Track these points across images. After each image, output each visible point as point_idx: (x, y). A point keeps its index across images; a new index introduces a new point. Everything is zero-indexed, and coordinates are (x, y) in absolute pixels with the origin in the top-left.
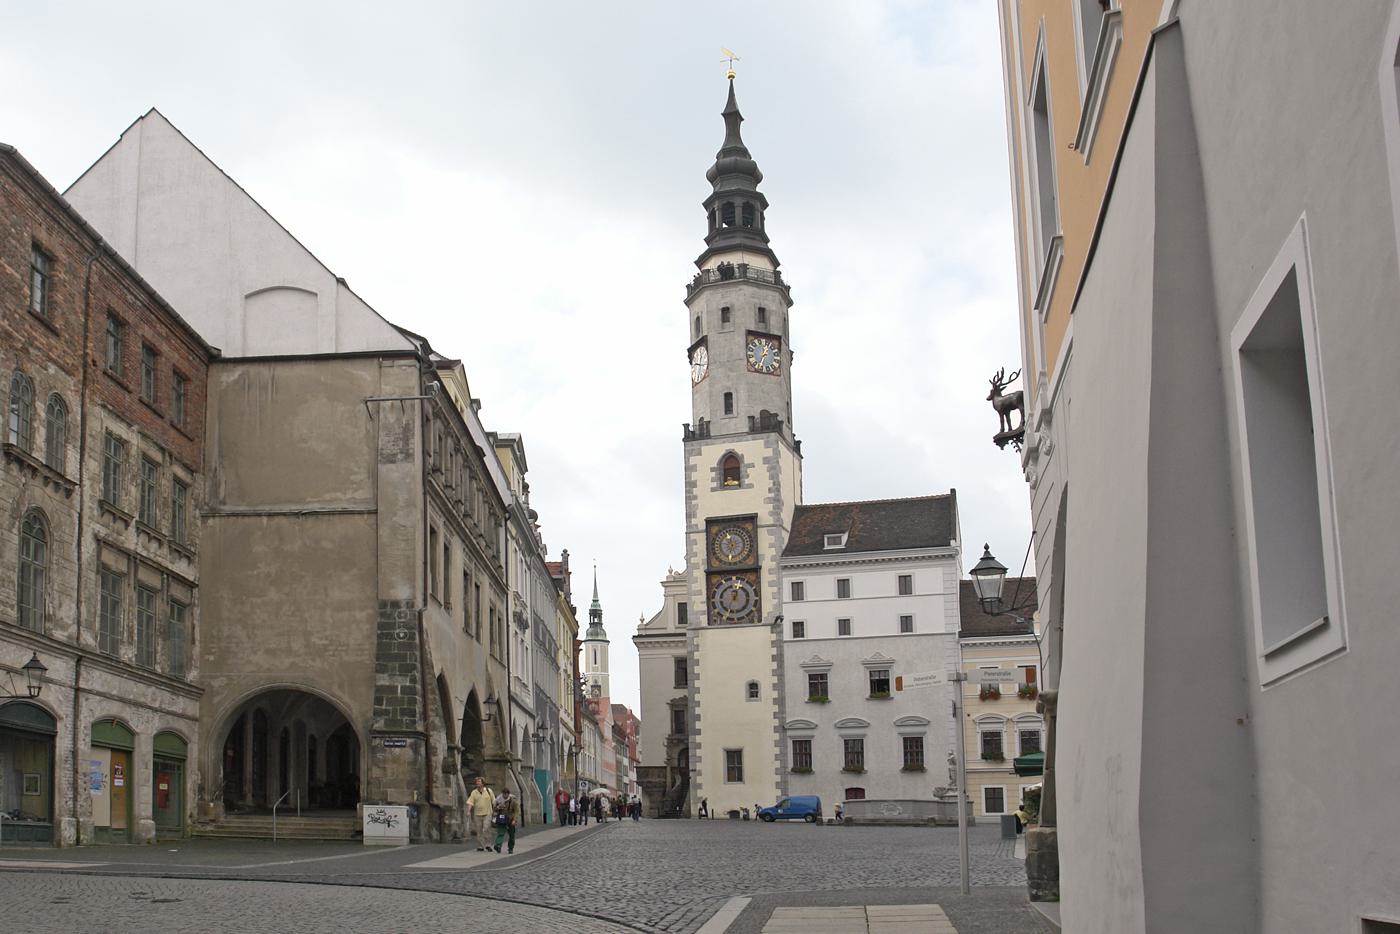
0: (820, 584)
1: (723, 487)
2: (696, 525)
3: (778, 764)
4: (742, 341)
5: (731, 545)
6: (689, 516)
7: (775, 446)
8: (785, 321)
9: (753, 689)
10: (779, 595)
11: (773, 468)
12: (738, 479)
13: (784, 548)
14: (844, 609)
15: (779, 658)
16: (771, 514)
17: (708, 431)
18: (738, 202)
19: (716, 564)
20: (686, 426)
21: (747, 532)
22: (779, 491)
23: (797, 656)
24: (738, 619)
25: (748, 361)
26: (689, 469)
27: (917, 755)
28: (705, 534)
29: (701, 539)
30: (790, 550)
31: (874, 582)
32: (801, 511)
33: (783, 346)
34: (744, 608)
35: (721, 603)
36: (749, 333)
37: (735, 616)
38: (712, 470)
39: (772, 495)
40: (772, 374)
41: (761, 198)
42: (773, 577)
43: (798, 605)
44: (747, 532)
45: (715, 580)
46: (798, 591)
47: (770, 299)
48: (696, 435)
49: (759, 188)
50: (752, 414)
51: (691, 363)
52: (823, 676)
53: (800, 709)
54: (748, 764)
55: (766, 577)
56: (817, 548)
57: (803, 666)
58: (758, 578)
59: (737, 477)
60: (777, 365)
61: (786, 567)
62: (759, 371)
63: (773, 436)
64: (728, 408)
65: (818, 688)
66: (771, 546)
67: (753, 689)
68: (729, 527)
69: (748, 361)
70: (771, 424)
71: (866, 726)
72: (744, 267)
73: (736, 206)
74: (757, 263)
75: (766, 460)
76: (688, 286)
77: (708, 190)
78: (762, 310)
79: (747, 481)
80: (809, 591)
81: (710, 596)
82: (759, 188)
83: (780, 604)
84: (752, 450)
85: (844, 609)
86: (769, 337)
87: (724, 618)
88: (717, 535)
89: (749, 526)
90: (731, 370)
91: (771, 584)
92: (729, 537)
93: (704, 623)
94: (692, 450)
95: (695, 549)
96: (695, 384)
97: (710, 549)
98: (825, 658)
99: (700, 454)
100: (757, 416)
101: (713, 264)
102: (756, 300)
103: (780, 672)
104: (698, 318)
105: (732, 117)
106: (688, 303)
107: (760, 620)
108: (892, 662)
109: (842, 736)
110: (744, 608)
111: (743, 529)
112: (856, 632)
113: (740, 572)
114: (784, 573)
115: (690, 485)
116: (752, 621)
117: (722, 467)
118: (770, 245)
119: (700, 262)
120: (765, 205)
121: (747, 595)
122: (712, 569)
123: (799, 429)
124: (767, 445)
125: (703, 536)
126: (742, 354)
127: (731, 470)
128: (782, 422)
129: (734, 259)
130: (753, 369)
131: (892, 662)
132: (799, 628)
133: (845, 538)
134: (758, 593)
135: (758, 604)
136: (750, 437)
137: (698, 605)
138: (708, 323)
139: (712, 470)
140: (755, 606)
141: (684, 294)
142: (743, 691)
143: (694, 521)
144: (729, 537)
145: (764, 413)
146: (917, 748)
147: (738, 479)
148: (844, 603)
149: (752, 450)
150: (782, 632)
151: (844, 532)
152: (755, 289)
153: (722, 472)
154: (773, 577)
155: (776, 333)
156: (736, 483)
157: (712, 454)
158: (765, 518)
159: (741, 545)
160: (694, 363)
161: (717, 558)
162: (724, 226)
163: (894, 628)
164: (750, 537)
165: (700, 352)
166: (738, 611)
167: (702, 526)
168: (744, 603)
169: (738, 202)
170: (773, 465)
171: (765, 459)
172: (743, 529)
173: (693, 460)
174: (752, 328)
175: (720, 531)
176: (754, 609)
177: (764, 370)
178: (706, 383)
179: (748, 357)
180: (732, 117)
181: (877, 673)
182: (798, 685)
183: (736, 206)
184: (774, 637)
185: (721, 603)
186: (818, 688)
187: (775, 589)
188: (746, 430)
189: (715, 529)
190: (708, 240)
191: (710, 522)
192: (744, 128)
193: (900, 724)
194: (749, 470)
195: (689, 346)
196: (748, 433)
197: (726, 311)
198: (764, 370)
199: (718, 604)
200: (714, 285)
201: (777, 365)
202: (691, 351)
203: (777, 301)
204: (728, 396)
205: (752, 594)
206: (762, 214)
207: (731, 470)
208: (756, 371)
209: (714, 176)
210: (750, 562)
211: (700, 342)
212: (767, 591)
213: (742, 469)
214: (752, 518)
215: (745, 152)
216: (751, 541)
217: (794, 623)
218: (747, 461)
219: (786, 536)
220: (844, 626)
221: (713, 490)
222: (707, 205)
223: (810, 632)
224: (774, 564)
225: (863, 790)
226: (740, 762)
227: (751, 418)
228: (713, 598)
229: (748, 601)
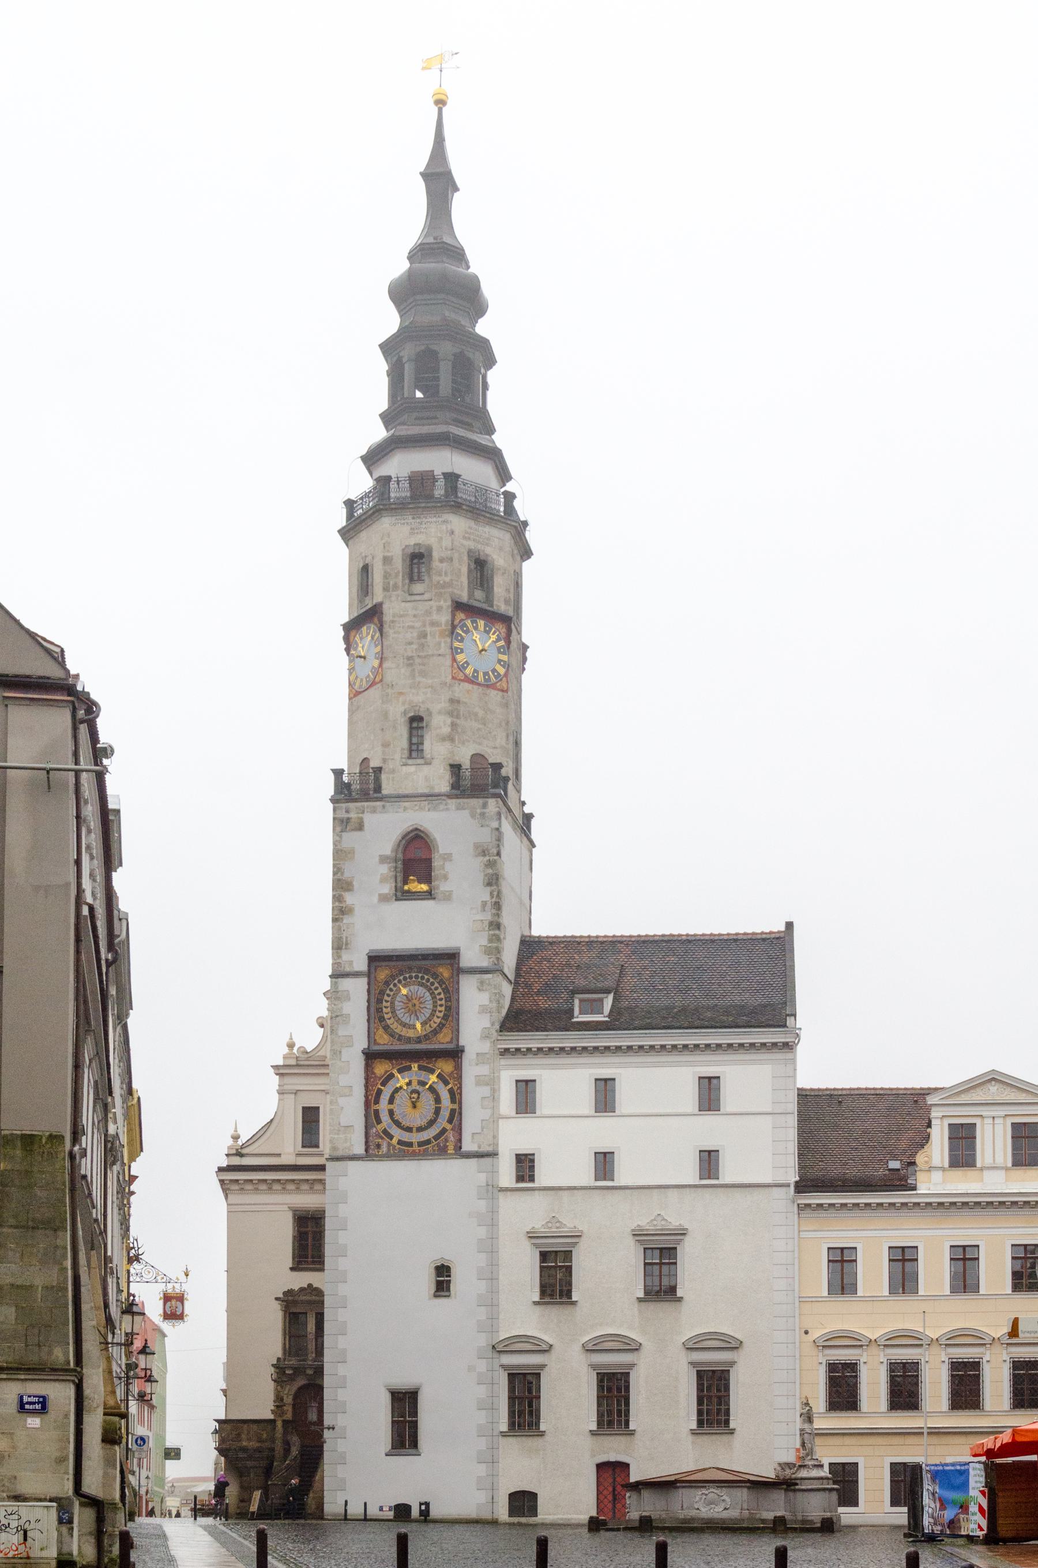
0: (566, 1084)
1: (403, 895)
2: (351, 963)
3: (482, 1418)
4: (445, 618)
5: (412, 1006)
6: (339, 945)
7: (495, 824)
8: (518, 586)
9: (443, 1279)
10: (494, 1097)
11: (491, 864)
12: (427, 878)
13: (504, 1012)
14: (604, 1133)
15: (491, 1220)
16: (487, 951)
17: (378, 788)
18: (446, 349)
19: (384, 1042)
20: (338, 773)
22: (498, 906)
23: (524, 1215)
24: (421, 1144)
25: (454, 660)
26: (340, 855)
27: (720, 1404)
28: (365, 980)
29: (358, 989)
30: (517, 1019)
31: (657, 1084)
32: (530, 946)
33: (514, 636)
34: (431, 1123)
35: (391, 1113)
36: (458, 606)
37: (415, 1138)
38: (383, 859)
40: (492, 686)
41: (484, 346)
42: (484, 1070)
43: (526, 1122)
45: (381, 1068)
46: (526, 1096)
47: (495, 544)
48: (357, 790)
49: (483, 328)
50: (457, 759)
51: (348, 650)
52: (568, 1255)
53: (523, 1315)
54: (429, 1420)
55: (471, 1070)
56: (561, 1020)
57: (532, 1236)
58: (458, 1068)
59: (427, 877)
60: (502, 671)
61: (507, 1050)
62: (470, 680)
63: (492, 802)
64: (415, 750)
65: (556, 1279)
66: (483, 1010)
67: (443, 1279)
68: (410, 969)
69: (454, 660)
70: (486, 782)
71: (634, 1348)
72: (452, 478)
73: (438, 355)
74: (473, 471)
76: (350, 504)
77: (389, 321)
78: (481, 568)
79: (442, 887)
80: (545, 1097)
81: (371, 1099)
82: (483, 328)
83: (496, 1118)
84: (453, 829)
85: (604, 1133)
86: (493, 617)
87: (394, 1141)
88: (387, 983)
89: (445, 972)
90: (424, 674)
91: (479, 1081)
92: (404, 991)
93: (359, 1149)
94: (348, 819)
95: (347, 1008)
96: (355, 694)
97: (372, 1009)
98: (569, 1223)
99: (360, 827)
100: (466, 764)
101: (400, 466)
102: (472, 545)
103: (490, 1247)
104: (366, 570)
105: (439, 182)
106: (347, 534)
107: (458, 1147)
108: (682, 1233)
109: (594, 1367)
110: (431, 1123)
111: (435, 976)
112: (623, 1176)
113: (427, 1057)
114: (503, 1062)
115: (341, 886)
116: (442, 1152)
117: (400, 856)
118: (499, 439)
119: (372, 458)
120: (490, 361)
121: (438, 1100)
122: (376, 1048)
123: (535, 790)
125: (363, 982)
126: (444, 649)
127: (415, 864)
128: (506, 779)
129: (438, 461)
130: (461, 676)
131: (682, 1233)
133: (608, 1002)
134: (456, 1096)
135: (456, 1117)
136: (452, 803)
137: (345, 1116)
138: (386, 576)
139: (383, 859)
140: (450, 1121)
141: (341, 520)
142: (427, 1281)
143: (345, 956)
144: (404, 991)
145: (477, 758)
146: (719, 1390)
147: (427, 878)
148: (605, 1122)
149: (453, 829)
150: (494, 1172)
151: (607, 991)
152: (472, 523)
153: (400, 865)
154: (484, 1070)
155: (501, 606)
156: (424, 887)
157: (384, 829)
158: (470, 957)
159: (429, 1005)
160: (352, 652)
161: (386, 1028)
162: (419, 395)
163: (690, 1174)
164: (446, 991)
165: (368, 631)
166: (420, 1129)
167: (362, 965)
168: (430, 1116)
169: (446, 349)
170: (490, 856)
171: (476, 846)
172: (435, 976)
173: (351, 839)
174: (464, 597)
175: (393, 977)
176: (449, 1127)
177: (481, 679)
178: (375, 693)
179: (454, 651)
180: (439, 182)
181: (657, 1253)
182: (522, 1271)
183: (438, 355)
184: (482, 1178)
185: (391, 1113)
186: (556, 1279)
187: (486, 1091)
189: (382, 975)
190: (388, 418)
191: (375, 959)
192: (458, 203)
193: (690, 1347)
195: (346, 619)
196: (449, 796)
197: (417, 560)
198: (481, 679)
199: (385, 1117)
200: (399, 508)
201: (502, 671)
202: (351, 628)
203: (508, 549)
204: (416, 722)
205: (445, 1096)
206: (484, 377)
207: (415, 864)
208: (467, 680)
209: (403, 293)
210: (443, 1041)
211: (366, 618)
212: (472, 1094)
213: (436, 863)
214: (451, 957)
215: (458, 254)
216: (448, 999)
217: (517, 1155)
219: (507, 990)
220: (604, 1163)
221: (383, 898)
222: (388, 348)
223: (544, 1176)
224: (486, 1047)
225: (628, 1465)
226: (414, 1412)
227: (456, 769)
228: (377, 1102)
229: (437, 1111)
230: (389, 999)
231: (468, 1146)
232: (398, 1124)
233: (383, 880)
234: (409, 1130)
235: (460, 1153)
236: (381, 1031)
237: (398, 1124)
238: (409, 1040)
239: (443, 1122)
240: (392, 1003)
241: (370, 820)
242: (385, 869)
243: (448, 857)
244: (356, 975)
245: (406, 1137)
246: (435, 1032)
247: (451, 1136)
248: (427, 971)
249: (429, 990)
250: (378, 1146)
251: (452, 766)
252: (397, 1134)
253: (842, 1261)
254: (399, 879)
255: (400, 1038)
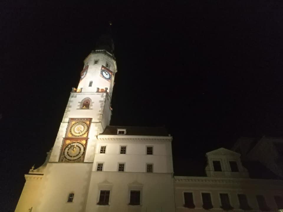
19: (70, 136)
21: (87, 125)
38: (79, 102)
39: (100, 113)
44: (87, 125)
68: (80, 122)
75: (100, 101)
79: (91, 107)
99: (76, 97)
111: (85, 123)
116: (79, 162)
124: (102, 96)
125: (67, 124)
132: (100, 167)
135: (84, 153)
139: (79, 102)
140: (82, 155)
153: (82, 104)
161: (71, 133)
164: (87, 126)
166: (74, 157)
172: (85, 123)
185: (68, 152)
188: (96, 91)
194: (93, 104)
218: (92, 101)
221: (78, 109)
227: (98, 89)
230: (74, 128)
231: (85, 161)
232: (69, 155)
233: (78, 106)
234: (71, 157)
235: (83, 162)
236: (70, 134)
237: (69, 155)
238: (76, 136)
239: (80, 155)
240: (74, 128)
241: (78, 96)
242: (79, 104)
243: (93, 102)
244: (67, 122)
245: (70, 158)
246: (83, 135)
247: (82, 159)
248: (84, 122)
249: (83, 126)
250: (62, 160)
251: (97, 88)
252: (68, 157)
253: (188, 197)
254: (82, 106)
255: (74, 136)
